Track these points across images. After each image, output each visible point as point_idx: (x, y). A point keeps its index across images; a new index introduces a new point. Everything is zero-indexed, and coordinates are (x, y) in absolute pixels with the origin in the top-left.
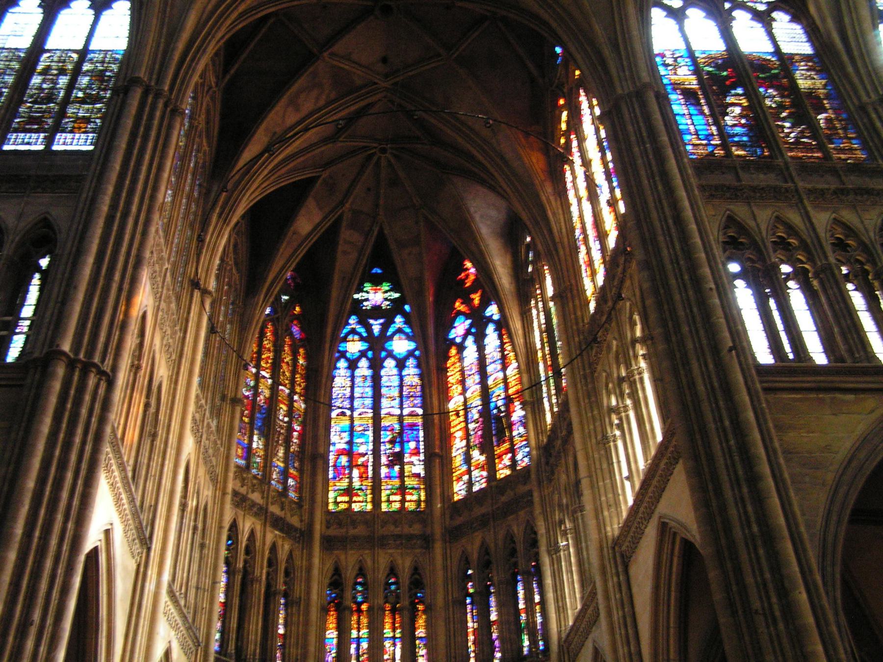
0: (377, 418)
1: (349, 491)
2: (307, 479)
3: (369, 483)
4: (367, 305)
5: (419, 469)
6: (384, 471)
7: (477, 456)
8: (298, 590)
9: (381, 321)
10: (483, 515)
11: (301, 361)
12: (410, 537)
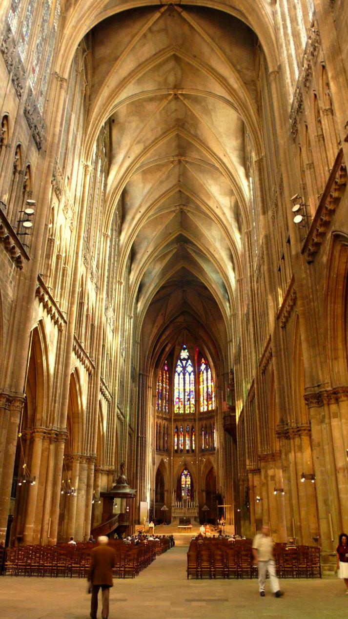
0: (184, 390)
1: (179, 408)
2: (170, 405)
3: (183, 406)
4: (182, 357)
5: (194, 403)
6: (186, 403)
7: (206, 403)
8: (169, 432)
9: (185, 362)
10: (206, 417)
11: (168, 376)
12: (191, 419)
